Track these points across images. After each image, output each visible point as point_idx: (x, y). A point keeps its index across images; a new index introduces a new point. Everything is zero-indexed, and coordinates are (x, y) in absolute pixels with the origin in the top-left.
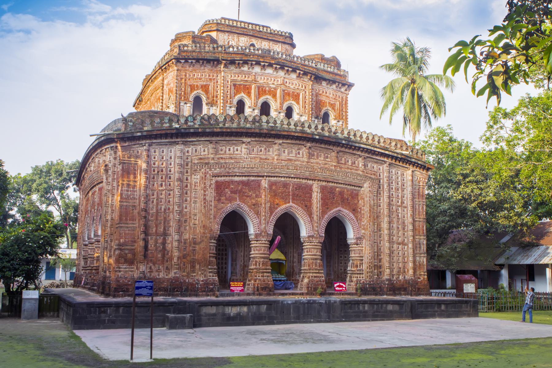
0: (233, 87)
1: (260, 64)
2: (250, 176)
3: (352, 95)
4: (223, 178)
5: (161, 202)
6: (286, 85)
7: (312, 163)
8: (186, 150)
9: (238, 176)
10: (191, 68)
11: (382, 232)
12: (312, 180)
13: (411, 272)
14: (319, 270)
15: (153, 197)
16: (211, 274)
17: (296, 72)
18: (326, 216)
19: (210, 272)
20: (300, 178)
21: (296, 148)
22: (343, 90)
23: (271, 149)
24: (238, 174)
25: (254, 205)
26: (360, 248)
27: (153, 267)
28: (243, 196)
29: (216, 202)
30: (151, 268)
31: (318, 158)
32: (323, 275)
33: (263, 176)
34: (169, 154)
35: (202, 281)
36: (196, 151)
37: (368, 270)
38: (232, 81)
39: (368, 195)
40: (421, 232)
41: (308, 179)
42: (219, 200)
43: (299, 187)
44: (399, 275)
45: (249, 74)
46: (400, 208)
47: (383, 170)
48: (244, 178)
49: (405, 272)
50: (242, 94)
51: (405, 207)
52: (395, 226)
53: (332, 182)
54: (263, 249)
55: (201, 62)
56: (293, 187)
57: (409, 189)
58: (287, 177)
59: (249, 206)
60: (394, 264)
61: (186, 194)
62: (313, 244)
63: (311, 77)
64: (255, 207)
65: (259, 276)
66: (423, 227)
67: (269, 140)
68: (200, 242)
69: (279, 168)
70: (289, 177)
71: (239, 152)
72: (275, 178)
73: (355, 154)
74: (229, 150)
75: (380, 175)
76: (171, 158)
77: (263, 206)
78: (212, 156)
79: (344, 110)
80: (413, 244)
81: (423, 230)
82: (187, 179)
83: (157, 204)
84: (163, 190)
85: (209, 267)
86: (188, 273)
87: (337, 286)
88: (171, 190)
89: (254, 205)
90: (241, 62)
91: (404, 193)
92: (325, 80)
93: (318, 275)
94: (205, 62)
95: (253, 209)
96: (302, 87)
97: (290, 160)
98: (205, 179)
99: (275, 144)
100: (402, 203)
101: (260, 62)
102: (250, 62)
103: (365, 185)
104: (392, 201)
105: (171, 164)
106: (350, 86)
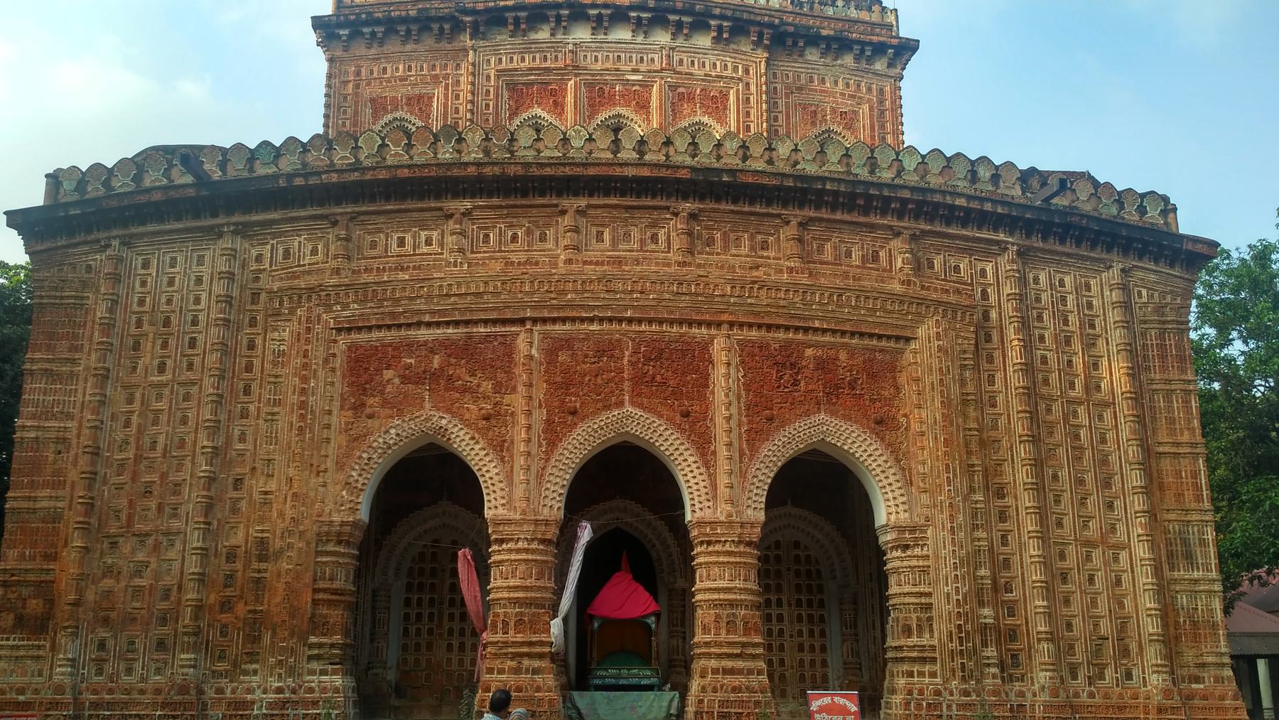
0: (506, 94)
1: (587, 18)
2: (476, 322)
3: (916, 82)
4: (375, 335)
5: (156, 422)
6: (679, 69)
7: (699, 266)
8: (254, 253)
9: (429, 325)
10: (373, 51)
11: (1009, 501)
12: (709, 325)
13: (1153, 655)
14: (744, 645)
15: (129, 408)
16: (315, 665)
17: (708, 27)
18: (765, 450)
19: (310, 658)
20: (661, 322)
21: (646, 222)
22: (880, 65)
23: (550, 233)
24: (427, 318)
25: (487, 418)
26: (914, 563)
27: (110, 643)
28: (447, 390)
29: (350, 413)
30: (102, 645)
31: (726, 248)
32: (762, 665)
33: (522, 321)
34: (194, 268)
35: (279, 690)
36: (287, 254)
37: (955, 645)
38: (500, 74)
39: (935, 364)
40: (1189, 495)
41: (691, 324)
42: (358, 408)
43: (656, 352)
44: (1102, 668)
45: (556, 47)
46: (1081, 410)
47: (997, 275)
48: (450, 331)
49: (1125, 652)
50: (538, 111)
51: (1106, 405)
52: (1064, 474)
53: (787, 328)
54: (522, 567)
55: (402, 29)
56: (635, 353)
57: (1117, 336)
58: (610, 320)
59: (468, 424)
60: (1077, 622)
61: (247, 391)
62: (718, 547)
63: (761, 36)
64: (492, 424)
65: (501, 672)
66: (1195, 475)
67: (540, 201)
68: (281, 551)
69: (576, 291)
70: (620, 320)
71: (435, 247)
72: (568, 327)
73: (872, 227)
74: (401, 243)
75: (984, 293)
76: (199, 280)
77: (522, 420)
78: (334, 264)
79: (889, 127)
80: (1153, 545)
81: (1197, 488)
82: (251, 346)
83: (141, 430)
84: (162, 385)
85: (313, 639)
86: (235, 665)
87: (822, 710)
88: (193, 383)
89: (485, 419)
90: (523, 14)
91: (1094, 352)
92: (814, 40)
93: (740, 664)
94: (414, 27)
95: (483, 432)
96: (735, 69)
97: (619, 262)
98: (308, 341)
99: (563, 212)
100: (1092, 386)
101: (586, 6)
102: (554, 13)
103: (921, 332)
104: (1046, 382)
105: (197, 301)
106: (907, 48)
